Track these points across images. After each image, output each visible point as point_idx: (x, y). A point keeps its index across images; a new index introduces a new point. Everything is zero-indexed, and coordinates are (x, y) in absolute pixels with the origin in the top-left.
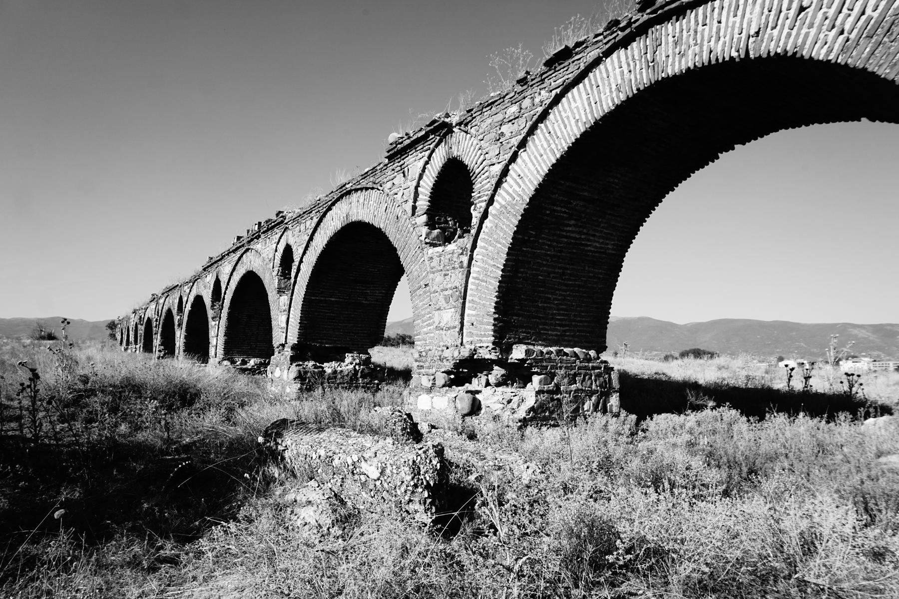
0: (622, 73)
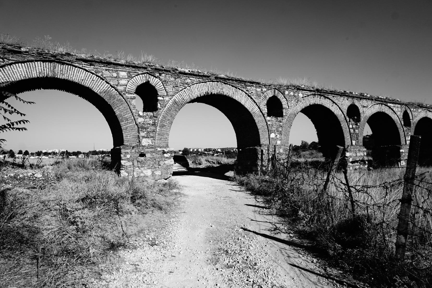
0: (41, 69)
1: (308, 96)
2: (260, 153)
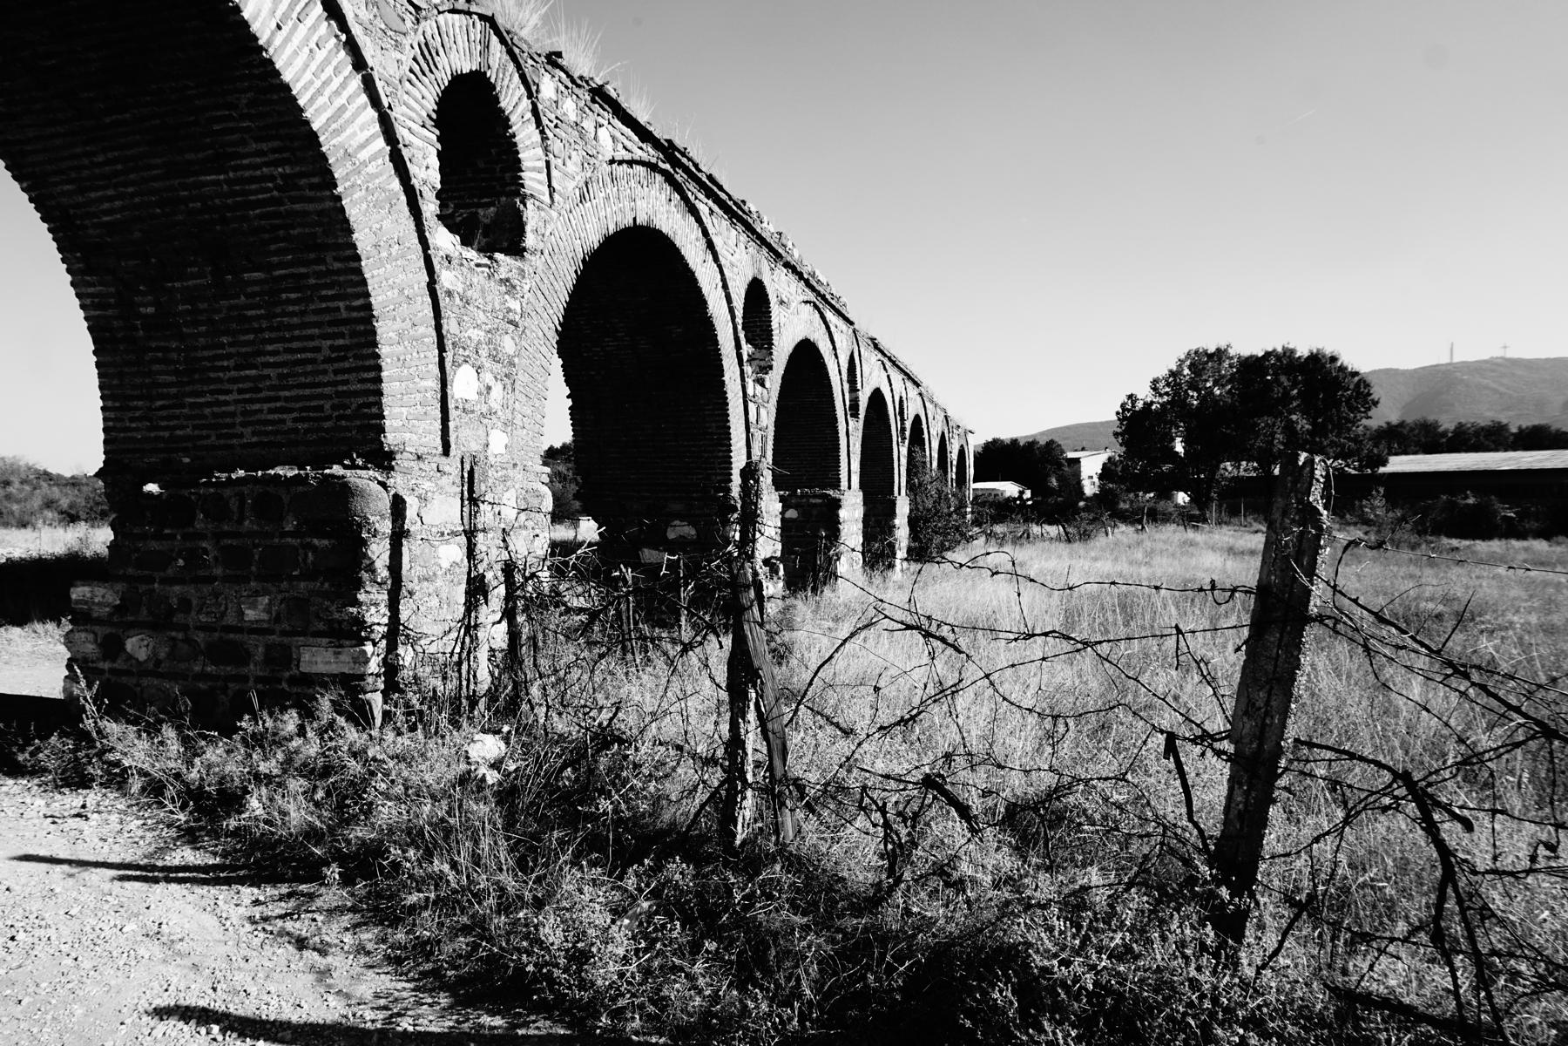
1: (631, 163)
2: (386, 527)
